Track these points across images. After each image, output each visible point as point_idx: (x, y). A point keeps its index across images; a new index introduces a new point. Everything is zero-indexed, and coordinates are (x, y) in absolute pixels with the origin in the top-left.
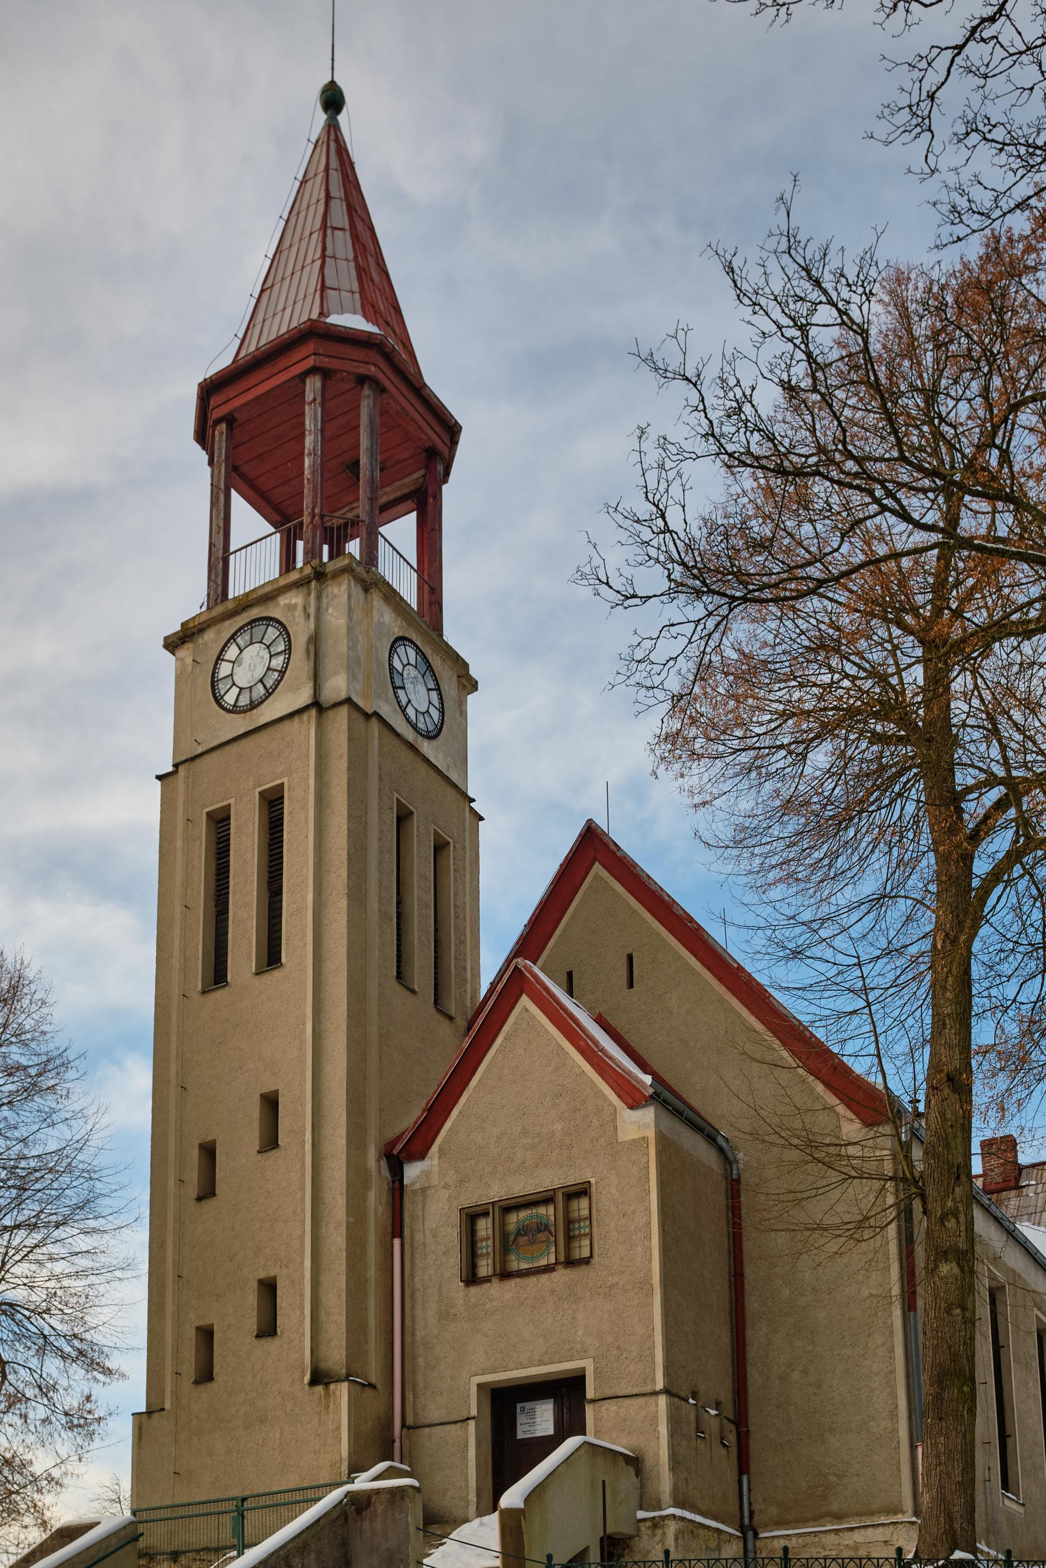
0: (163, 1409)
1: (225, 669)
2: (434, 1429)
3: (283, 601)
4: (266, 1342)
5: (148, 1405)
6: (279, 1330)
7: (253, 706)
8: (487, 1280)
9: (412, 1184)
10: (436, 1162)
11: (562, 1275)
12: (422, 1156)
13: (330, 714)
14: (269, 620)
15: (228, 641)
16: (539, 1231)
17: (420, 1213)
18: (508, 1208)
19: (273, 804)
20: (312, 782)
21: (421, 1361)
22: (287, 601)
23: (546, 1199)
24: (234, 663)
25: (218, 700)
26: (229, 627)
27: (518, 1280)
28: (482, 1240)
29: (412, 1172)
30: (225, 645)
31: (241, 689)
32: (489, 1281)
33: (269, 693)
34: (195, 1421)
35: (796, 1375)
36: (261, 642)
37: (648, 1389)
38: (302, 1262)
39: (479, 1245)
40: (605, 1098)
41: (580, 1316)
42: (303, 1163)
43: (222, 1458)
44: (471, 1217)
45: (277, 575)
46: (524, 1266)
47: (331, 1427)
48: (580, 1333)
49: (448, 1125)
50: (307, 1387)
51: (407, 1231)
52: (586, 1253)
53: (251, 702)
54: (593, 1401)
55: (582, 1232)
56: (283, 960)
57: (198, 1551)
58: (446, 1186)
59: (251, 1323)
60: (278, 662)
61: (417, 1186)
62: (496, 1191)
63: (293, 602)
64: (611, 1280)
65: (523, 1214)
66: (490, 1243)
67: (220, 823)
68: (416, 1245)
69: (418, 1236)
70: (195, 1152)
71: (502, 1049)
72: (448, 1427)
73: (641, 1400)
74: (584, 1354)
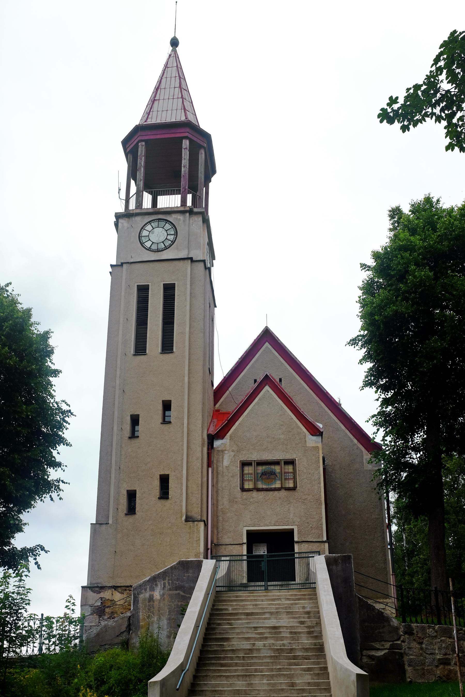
0: (107, 524)
1: (145, 233)
2: (228, 546)
3: (174, 216)
4: (163, 501)
5: (97, 520)
6: (170, 497)
7: (158, 251)
8: (249, 490)
9: (218, 447)
10: (228, 441)
11: (283, 493)
12: (222, 438)
13: (197, 264)
14: (167, 221)
15: (147, 223)
16: (272, 474)
17: (221, 460)
18: (260, 463)
19: (169, 290)
20: (188, 286)
21: (220, 518)
22: (176, 217)
23: (277, 463)
24: (150, 232)
25: (142, 244)
26: (148, 219)
27: (265, 492)
28: (246, 474)
29: (217, 443)
30: (146, 224)
31: (153, 243)
32: (252, 491)
33: (166, 248)
34: (125, 530)
35: (347, 544)
36: (163, 228)
37: (320, 540)
38: (182, 471)
39: (245, 476)
40: (301, 430)
41: (292, 509)
42: (183, 431)
43: (139, 547)
44: (244, 464)
45: (179, 205)
46: (264, 487)
47: (195, 539)
48: (292, 515)
49: (234, 428)
50: (184, 522)
51: (215, 466)
52: (291, 485)
53: (158, 249)
54: (298, 542)
55: (290, 477)
56: (174, 350)
57: (128, 587)
58: (233, 451)
59: (156, 491)
60: (171, 238)
61: (220, 449)
62: (255, 456)
63: (179, 217)
64: (304, 497)
65: (264, 467)
66: (253, 476)
67: (143, 291)
68: (219, 472)
69: (220, 469)
70: (129, 418)
71: (258, 403)
72: (234, 546)
73: (318, 544)
74: (293, 523)
